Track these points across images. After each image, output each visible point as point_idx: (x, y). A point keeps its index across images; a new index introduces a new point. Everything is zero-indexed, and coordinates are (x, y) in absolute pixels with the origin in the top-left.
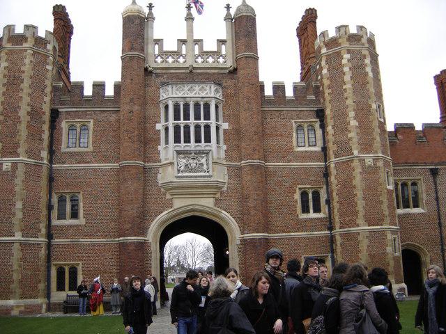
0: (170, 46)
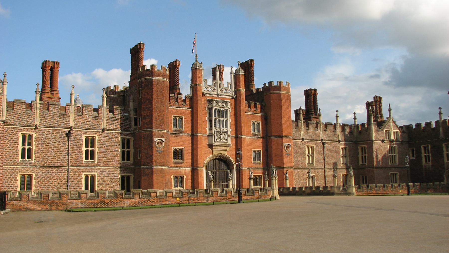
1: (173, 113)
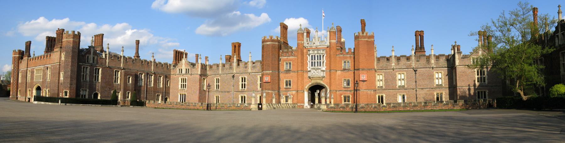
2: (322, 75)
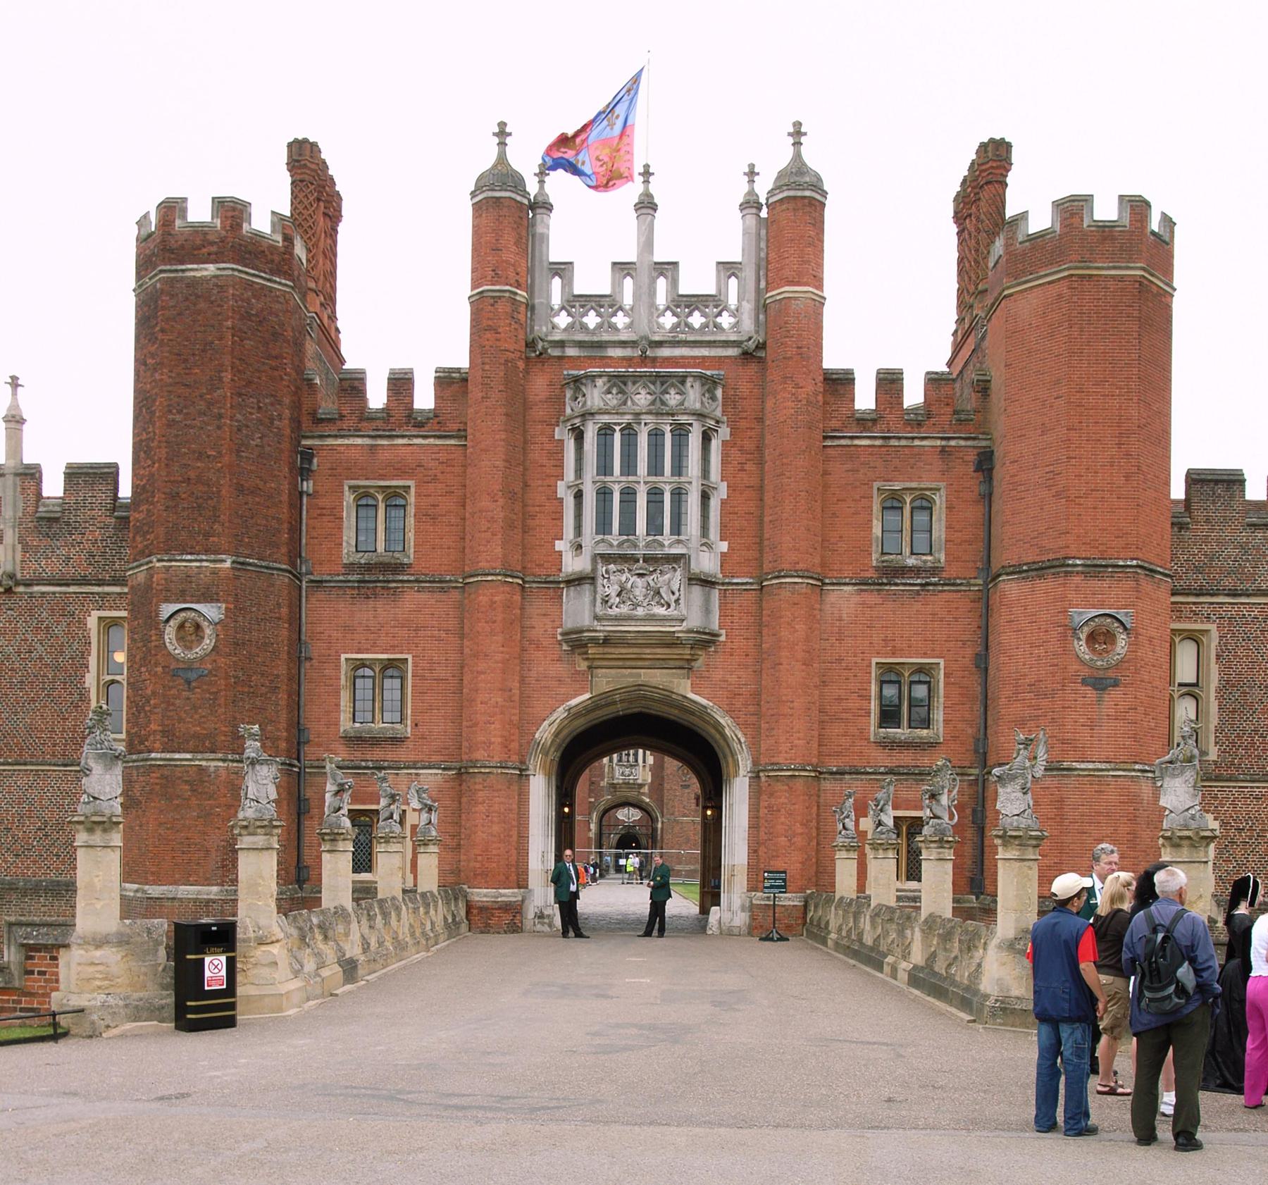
0: (592, 279)
1: (351, 470)
2: (695, 620)
